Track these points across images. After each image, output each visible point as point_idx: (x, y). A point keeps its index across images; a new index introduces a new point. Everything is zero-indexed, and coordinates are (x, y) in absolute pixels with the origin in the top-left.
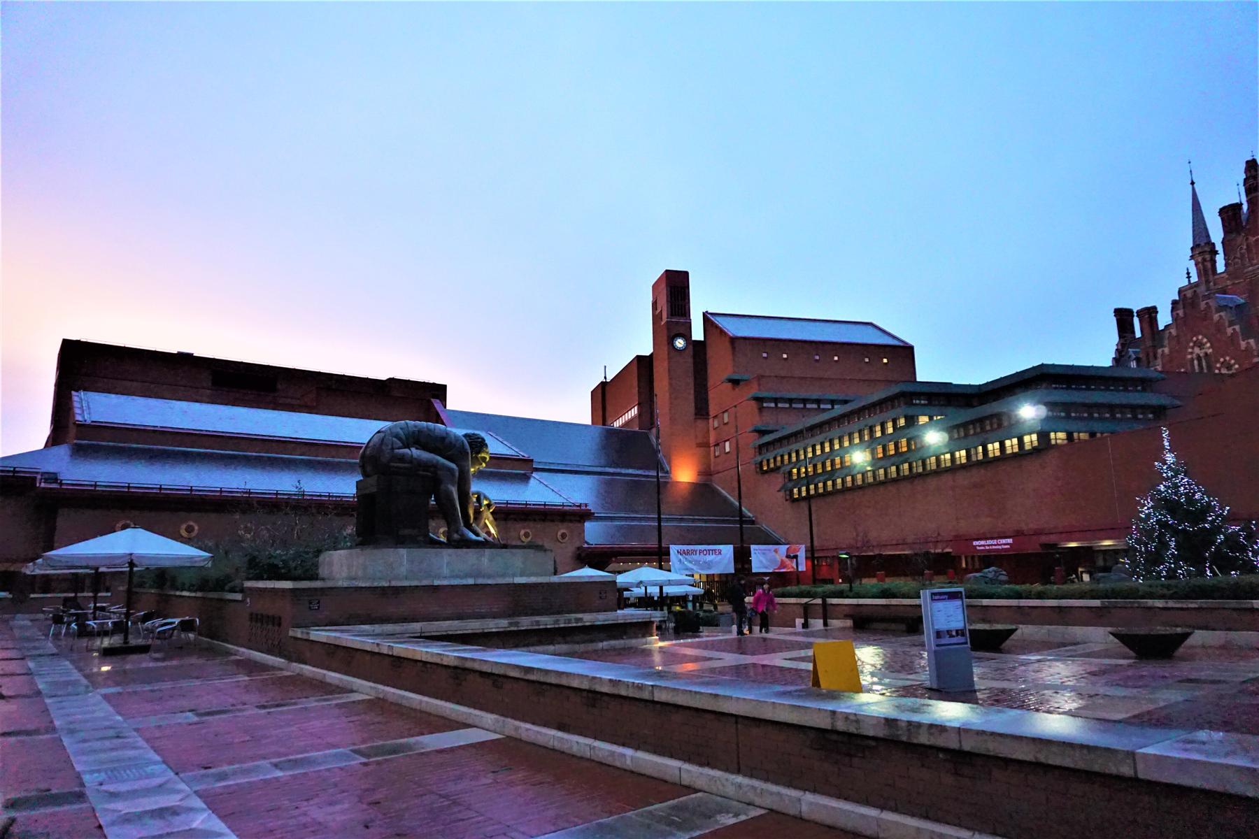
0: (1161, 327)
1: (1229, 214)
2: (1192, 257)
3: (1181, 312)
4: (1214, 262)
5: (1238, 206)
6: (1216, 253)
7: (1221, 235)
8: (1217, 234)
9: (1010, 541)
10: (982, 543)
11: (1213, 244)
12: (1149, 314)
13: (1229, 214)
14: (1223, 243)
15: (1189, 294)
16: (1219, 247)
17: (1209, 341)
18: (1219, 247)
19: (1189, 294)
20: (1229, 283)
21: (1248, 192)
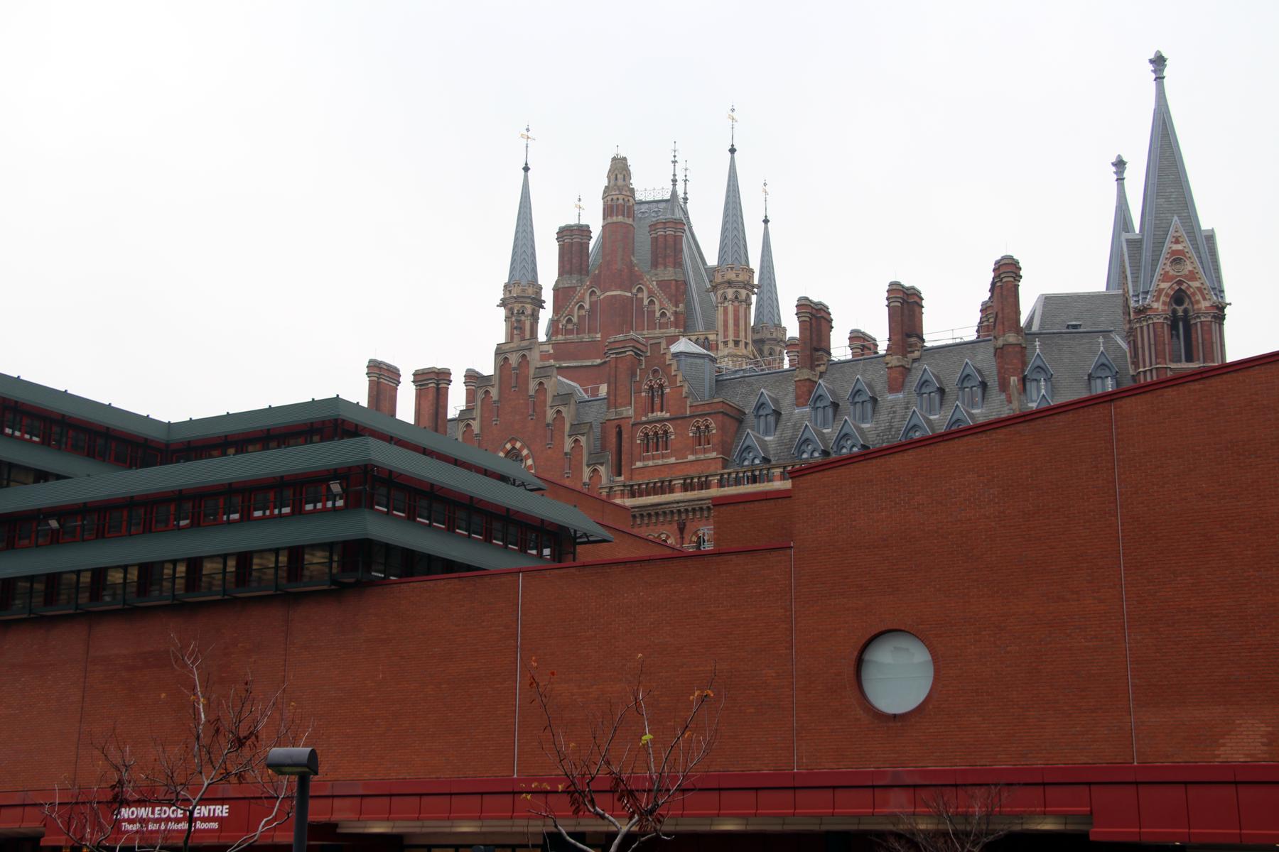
0: (452, 413)
1: (572, 238)
2: (503, 303)
3: (494, 393)
4: (535, 319)
5: (584, 231)
6: (539, 304)
7: (554, 275)
8: (548, 273)
9: (222, 810)
10: (143, 812)
11: (541, 288)
12: (432, 383)
13: (572, 238)
14: (556, 290)
15: (514, 359)
16: (548, 296)
17: (532, 454)
18: (548, 296)
19: (514, 359)
20: (552, 362)
21: (609, 211)
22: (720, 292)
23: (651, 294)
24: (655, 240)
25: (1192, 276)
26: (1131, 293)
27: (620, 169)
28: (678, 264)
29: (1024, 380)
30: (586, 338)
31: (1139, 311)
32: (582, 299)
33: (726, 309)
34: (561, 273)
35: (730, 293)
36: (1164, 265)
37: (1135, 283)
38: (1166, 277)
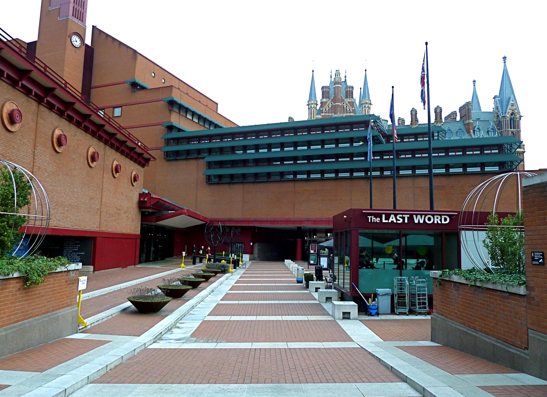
18: (319, 103)
22: (364, 105)
23: (346, 104)
24: (347, 92)
25: (516, 109)
26: (501, 112)
27: (338, 73)
28: (352, 98)
29: (474, 131)
30: (330, 114)
31: (503, 117)
32: (329, 104)
33: (365, 110)
34: (323, 98)
35: (367, 106)
36: (510, 106)
37: (502, 110)
38: (510, 109)
